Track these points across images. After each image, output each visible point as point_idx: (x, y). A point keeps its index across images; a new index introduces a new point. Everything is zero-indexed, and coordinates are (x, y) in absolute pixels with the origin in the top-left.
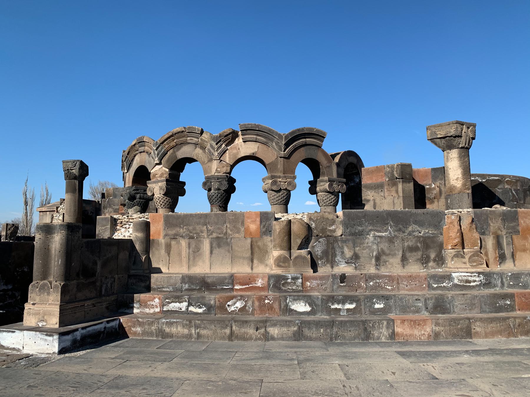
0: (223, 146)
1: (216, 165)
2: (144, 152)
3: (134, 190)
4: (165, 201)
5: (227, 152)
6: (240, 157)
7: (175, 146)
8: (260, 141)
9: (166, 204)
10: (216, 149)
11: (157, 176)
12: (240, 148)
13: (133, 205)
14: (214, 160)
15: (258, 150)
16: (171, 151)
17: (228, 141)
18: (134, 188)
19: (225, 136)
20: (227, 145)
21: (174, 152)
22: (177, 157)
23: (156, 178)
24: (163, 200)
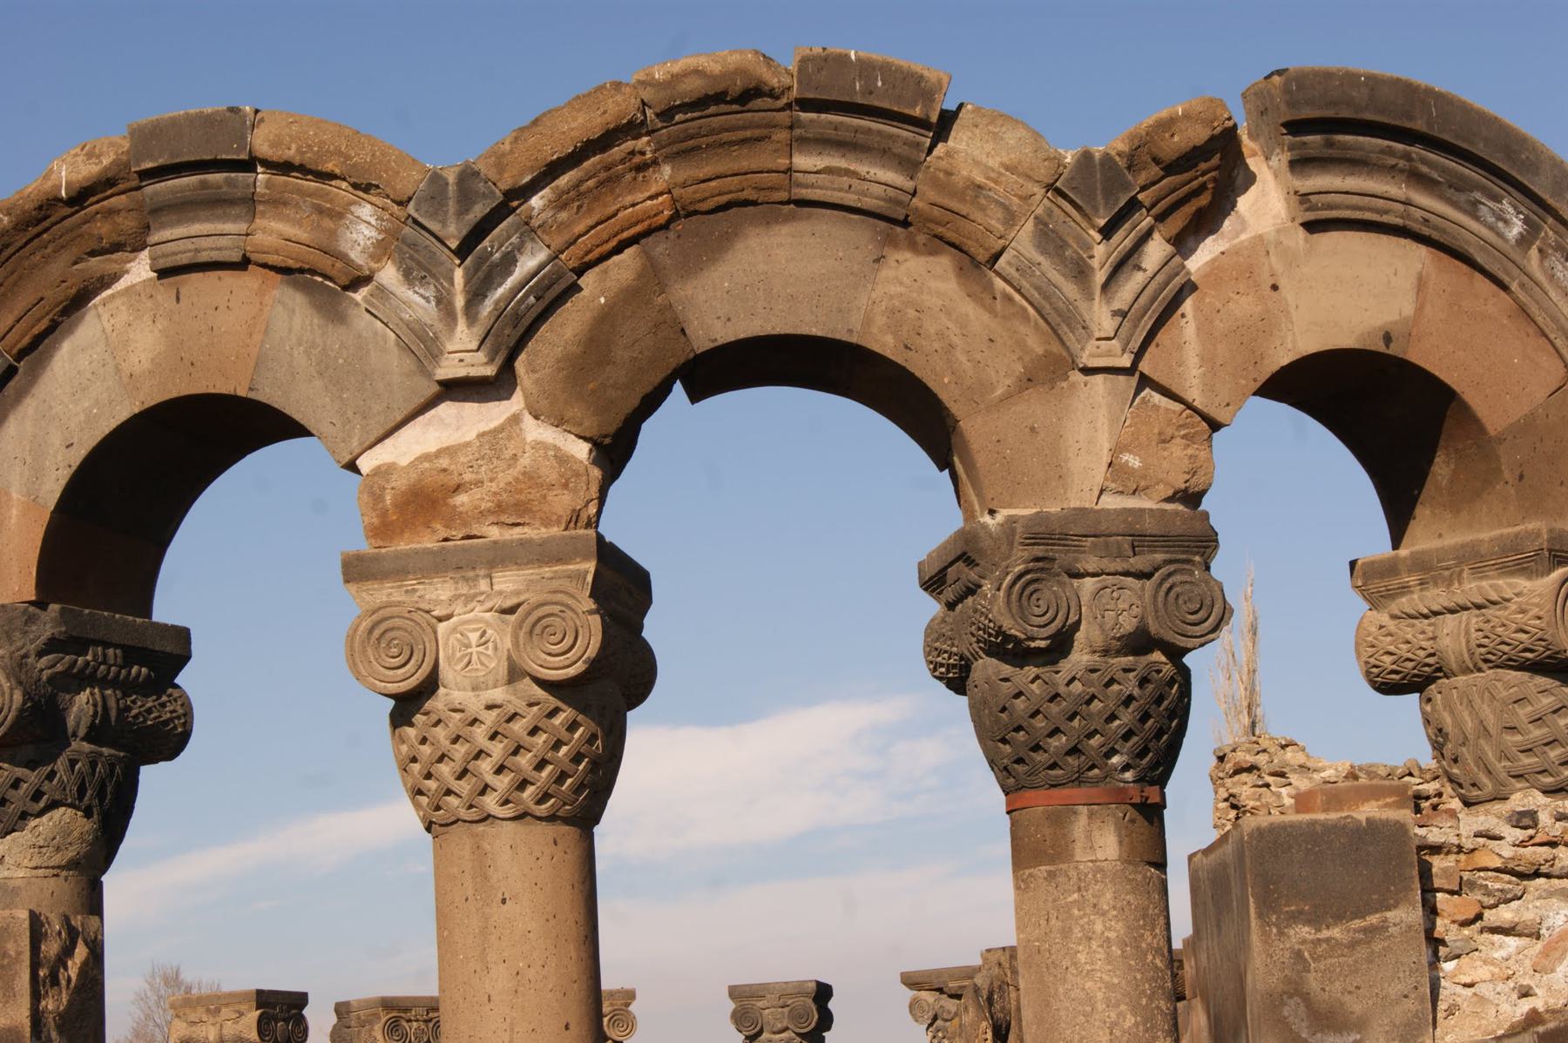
0: (1156, 251)
1: (1103, 411)
2: (243, 264)
3: (52, 646)
4: (558, 745)
5: (1188, 306)
6: (1285, 361)
7: (665, 226)
8: (1435, 235)
9: (561, 777)
10: (1100, 277)
11: (462, 499)
12: (1282, 283)
13: (37, 795)
14: (1076, 376)
15: (1420, 309)
16: (625, 266)
17: (1189, 209)
18: (49, 623)
19: (1170, 168)
20: (1183, 243)
21: (653, 278)
23: (453, 518)
24: (541, 739)
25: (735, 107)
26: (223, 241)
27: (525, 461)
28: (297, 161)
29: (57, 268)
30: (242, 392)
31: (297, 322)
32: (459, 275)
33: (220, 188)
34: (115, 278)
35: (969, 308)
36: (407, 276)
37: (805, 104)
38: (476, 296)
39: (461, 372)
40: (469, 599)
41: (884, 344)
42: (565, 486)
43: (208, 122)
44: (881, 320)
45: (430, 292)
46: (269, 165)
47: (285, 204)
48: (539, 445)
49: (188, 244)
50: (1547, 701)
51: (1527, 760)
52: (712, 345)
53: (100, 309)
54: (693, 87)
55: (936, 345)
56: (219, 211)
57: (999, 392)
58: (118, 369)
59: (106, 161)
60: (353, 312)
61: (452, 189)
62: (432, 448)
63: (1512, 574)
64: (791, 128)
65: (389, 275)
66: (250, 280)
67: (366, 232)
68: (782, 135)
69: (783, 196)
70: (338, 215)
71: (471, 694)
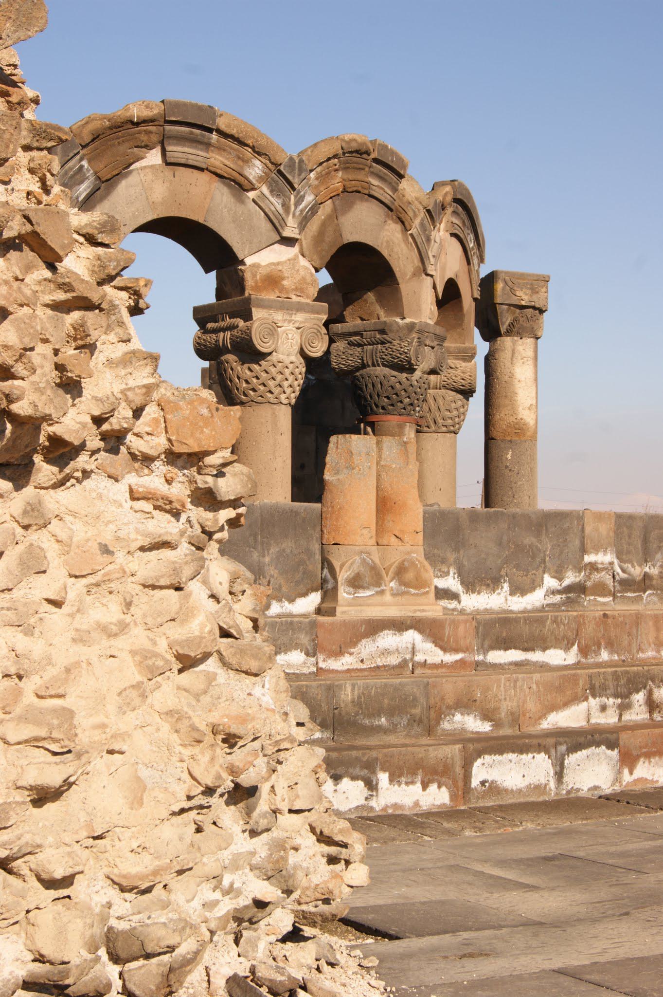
11: (285, 283)
21: (335, 214)
22: (344, 236)
23: (283, 289)
25: (359, 156)
26: (199, 158)
27: (302, 272)
28: (236, 136)
29: (122, 148)
30: (201, 221)
31: (225, 198)
32: (292, 197)
33: (197, 136)
34: (142, 158)
35: (403, 245)
36: (271, 192)
37: (376, 161)
38: (297, 204)
39: (292, 235)
40: (290, 321)
41: (385, 253)
42: (312, 284)
43: (200, 108)
44: (385, 244)
45: (280, 201)
46: (220, 132)
47: (224, 150)
48: (306, 268)
49: (184, 155)
50: (459, 403)
51: (450, 421)
52: (347, 242)
53: (140, 171)
54: (354, 146)
55: (396, 256)
56: (195, 145)
57: (408, 277)
58: (147, 199)
59: (155, 112)
60: (247, 201)
61: (297, 165)
62: (275, 261)
63: (458, 359)
64: (370, 167)
65: (265, 189)
66: (205, 177)
67: (258, 171)
68: (367, 169)
69: (367, 192)
70: (246, 161)
71: (285, 357)
